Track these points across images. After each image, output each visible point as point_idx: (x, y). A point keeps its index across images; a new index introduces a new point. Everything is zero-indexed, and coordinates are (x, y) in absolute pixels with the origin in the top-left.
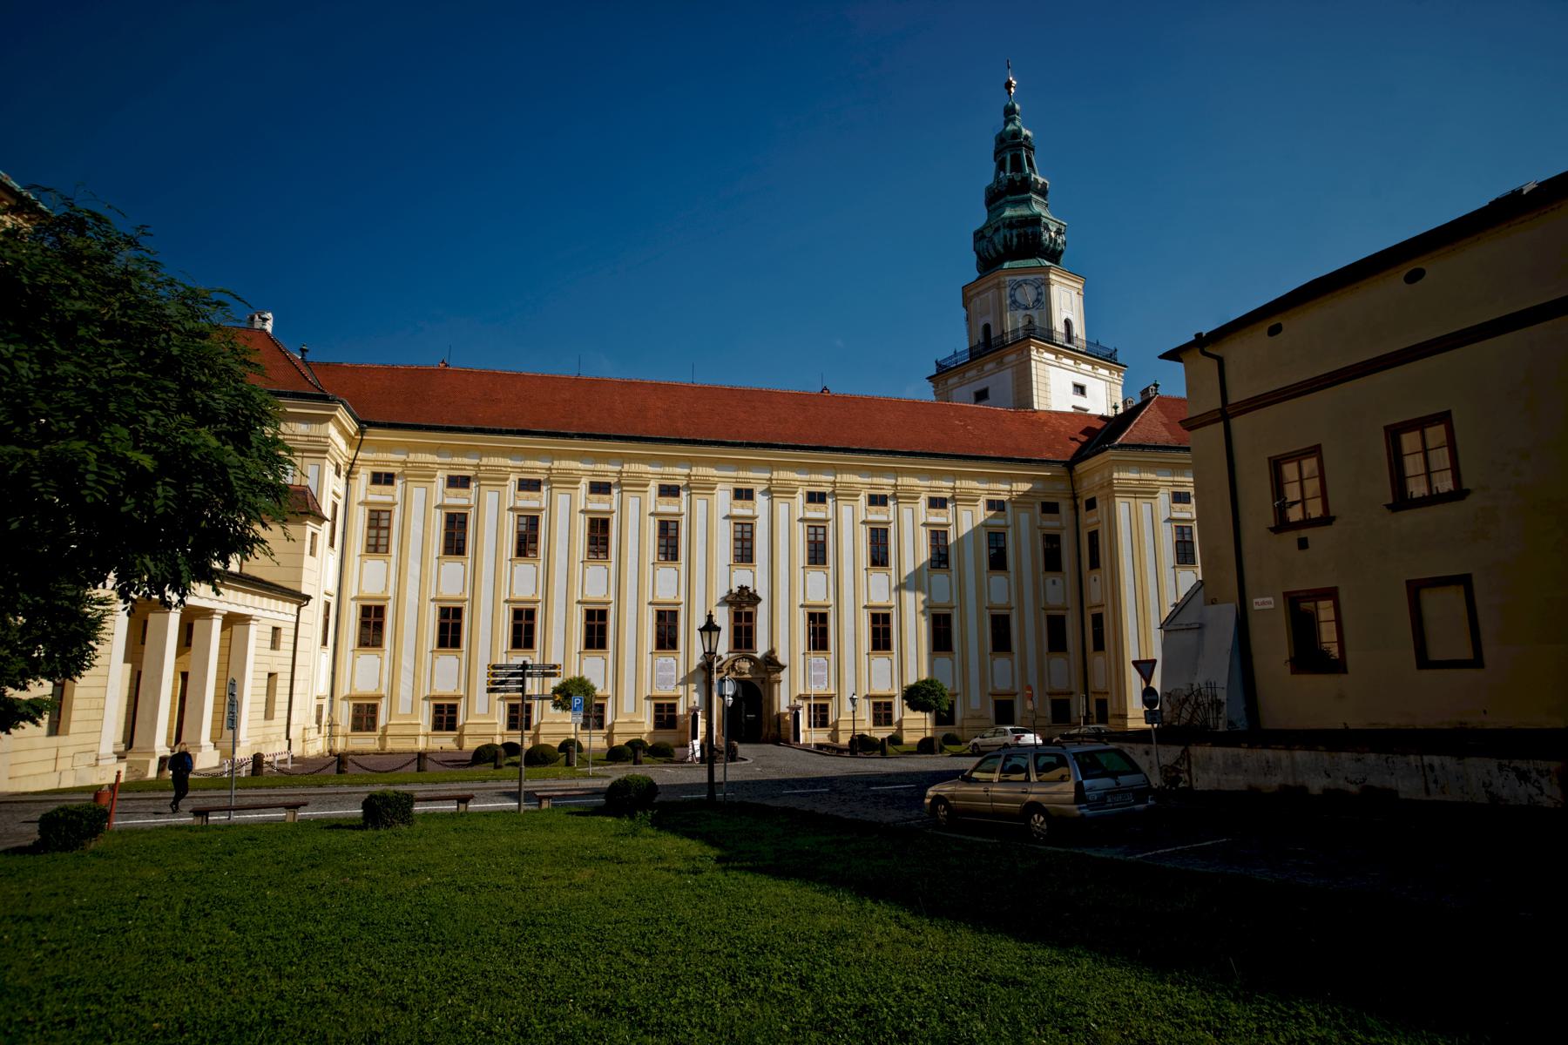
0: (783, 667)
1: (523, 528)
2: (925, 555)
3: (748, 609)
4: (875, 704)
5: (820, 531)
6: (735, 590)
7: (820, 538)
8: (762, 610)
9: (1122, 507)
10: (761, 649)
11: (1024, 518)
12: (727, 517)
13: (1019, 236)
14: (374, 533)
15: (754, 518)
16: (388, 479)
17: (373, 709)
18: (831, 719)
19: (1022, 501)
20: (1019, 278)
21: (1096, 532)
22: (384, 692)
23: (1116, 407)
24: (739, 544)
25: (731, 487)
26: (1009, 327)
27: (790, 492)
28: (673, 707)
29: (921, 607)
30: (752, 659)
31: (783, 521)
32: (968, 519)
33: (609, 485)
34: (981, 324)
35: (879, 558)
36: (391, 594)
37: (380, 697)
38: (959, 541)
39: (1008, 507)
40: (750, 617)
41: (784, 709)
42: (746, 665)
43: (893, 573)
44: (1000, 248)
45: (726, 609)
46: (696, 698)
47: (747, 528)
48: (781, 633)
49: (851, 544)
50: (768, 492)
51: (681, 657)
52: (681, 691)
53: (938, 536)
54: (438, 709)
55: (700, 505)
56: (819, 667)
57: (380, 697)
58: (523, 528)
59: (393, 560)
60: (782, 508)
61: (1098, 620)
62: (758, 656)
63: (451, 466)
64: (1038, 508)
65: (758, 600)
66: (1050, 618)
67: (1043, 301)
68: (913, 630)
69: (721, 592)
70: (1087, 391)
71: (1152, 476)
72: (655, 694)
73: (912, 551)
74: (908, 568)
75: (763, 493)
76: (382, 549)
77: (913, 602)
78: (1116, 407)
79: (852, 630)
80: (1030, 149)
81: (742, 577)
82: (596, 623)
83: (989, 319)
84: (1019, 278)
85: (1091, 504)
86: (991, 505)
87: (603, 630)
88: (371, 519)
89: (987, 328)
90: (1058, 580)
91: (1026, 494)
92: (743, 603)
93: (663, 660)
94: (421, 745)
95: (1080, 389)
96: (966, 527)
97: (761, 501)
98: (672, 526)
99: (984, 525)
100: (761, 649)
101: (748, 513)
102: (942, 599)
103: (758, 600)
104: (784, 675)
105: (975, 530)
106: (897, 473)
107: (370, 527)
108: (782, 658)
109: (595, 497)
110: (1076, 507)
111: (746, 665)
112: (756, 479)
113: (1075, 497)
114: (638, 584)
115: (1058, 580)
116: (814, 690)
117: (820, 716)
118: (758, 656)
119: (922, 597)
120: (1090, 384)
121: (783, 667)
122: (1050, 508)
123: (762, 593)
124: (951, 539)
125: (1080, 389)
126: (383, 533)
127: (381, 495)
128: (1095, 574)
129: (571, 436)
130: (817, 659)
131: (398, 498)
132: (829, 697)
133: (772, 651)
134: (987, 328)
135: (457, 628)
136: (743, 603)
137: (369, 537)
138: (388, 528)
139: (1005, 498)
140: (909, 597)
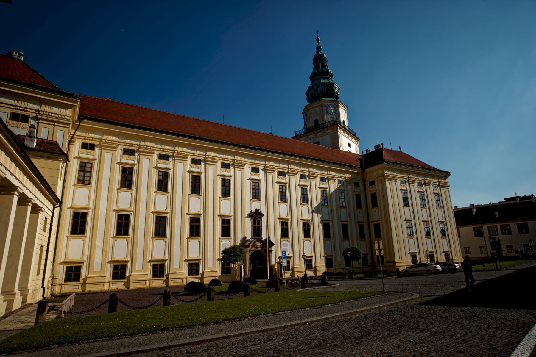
1: (161, 177)
2: (320, 200)
3: (258, 219)
5: (284, 187)
6: (254, 211)
7: (284, 190)
8: (264, 219)
9: (388, 183)
11: (350, 187)
12: (249, 179)
13: (327, 89)
14: (82, 174)
15: (259, 180)
16: (92, 147)
17: (78, 269)
19: (348, 181)
20: (329, 104)
21: (375, 194)
22: (85, 259)
23: (363, 152)
24: (254, 191)
25: (250, 166)
26: (326, 119)
27: (273, 171)
29: (320, 220)
30: (261, 241)
31: (270, 182)
32: (333, 186)
33: (200, 160)
34: (314, 118)
35: (305, 200)
36: (91, 206)
37: (82, 262)
38: (330, 195)
39: (345, 183)
40: (259, 223)
43: (310, 206)
44: (320, 93)
45: (250, 219)
47: (257, 184)
48: (271, 230)
49: (295, 194)
50: (265, 170)
53: (323, 191)
54: (115, 268)
55: (238, 173)
57: (82, 262)
58: (161, 177)
59: (93, 189)
60: (270, 177)
61: (377, 227)
62: (263, 239)
63: (126, 144)
64: (353, 184)
65: (263, 215)
66: (359, 225)
67: (337, 113)
68: (318, 229)
69: (248, 212)
70: (351, 146)
71: (395, 174)
73: (316, 199)
74: (315, 205)
75: (262, 170)
76: (87, 182)
77: (317, 217)
78: (363, 152)
79: (297, 229)
80: (327, 61)
81: (256, 205)
82: (195, 224)
83: (318, 117)
84: (329, 104)
85: (372, 183)
86: (339, 182)
87: (198, 227)
88: (80, 166)
89: (316, 121)
90: (361, 211)
91: (350, 179)
92: (256, 217)
94: (106, 287)
95: (350, 145)
96: (332, 190)
97: (262, 173)
98: (227, 181)
99: (338, 189)
100: (264, 237)
101: (257, 178)
102: (326, 217)
103: (263, 215)
104: (273, 248)
105: (335, 191)
106: (309, 166)
107: (80, 171)
109: (194, 165)
110: (364, 185)
111: (259, 244)
112: (260, 164)
113: (364, 181)
114: (214, 207)
115: (361, 211)
118: (263, 239)
119: (320, 216)
120: (353, 145)
121: (273, 244)
122: (357, 184)
123: (264, 212)
124: (328, 194)
125: (350, 145)
126: (88, 174)
127: (87, 154)
128: (375, 209)
129: (185, 136)
130: (285, 241)
131: (97, 156)
133: (269, 238)
134: (316, 121)
135: (127, 226)
136: (256, 217)
137: (79, 176)
138: (90, 172)
139: (344, 179)
140: (315, 215)
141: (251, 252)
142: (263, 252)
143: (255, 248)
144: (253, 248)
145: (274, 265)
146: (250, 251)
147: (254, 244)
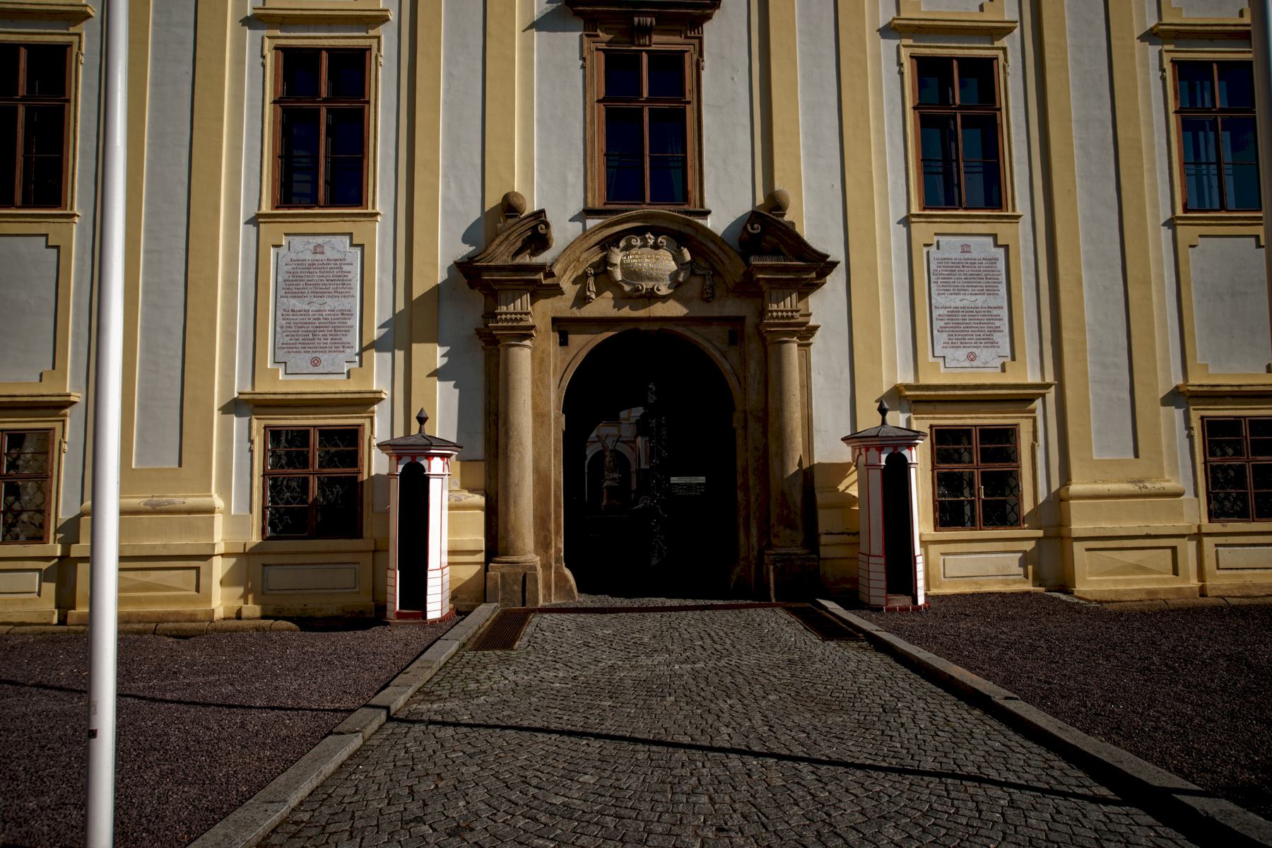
0: (822, 265)
3: (662, 42)
4: (1213, 428)
10: (725, 202)
18: (1032, 489)
28: (346, 444)
40: (674, 76)
41: (830, 447)
42: (660, 263)
45: (571, 40)
46: (443, 409)
51: (380, 234)
52: (379, 375)
56: (966, 274)
62: (717, 223)
72: (265, 387)
93: (302, 248)
100: (725, 202)
104: (824, 306)
108: (814, 223)
116: (951, 367)
117: (981, 478)
118: (717, 223)
121: (822, 265)
130: (962, 240)
132: (1020, 399)
141: (582, 343)
142: (711, 342)
143: (622, 299)
144: (602, 306)
145: (840, 470)
146: (564, 328)
147: (602, 270)
